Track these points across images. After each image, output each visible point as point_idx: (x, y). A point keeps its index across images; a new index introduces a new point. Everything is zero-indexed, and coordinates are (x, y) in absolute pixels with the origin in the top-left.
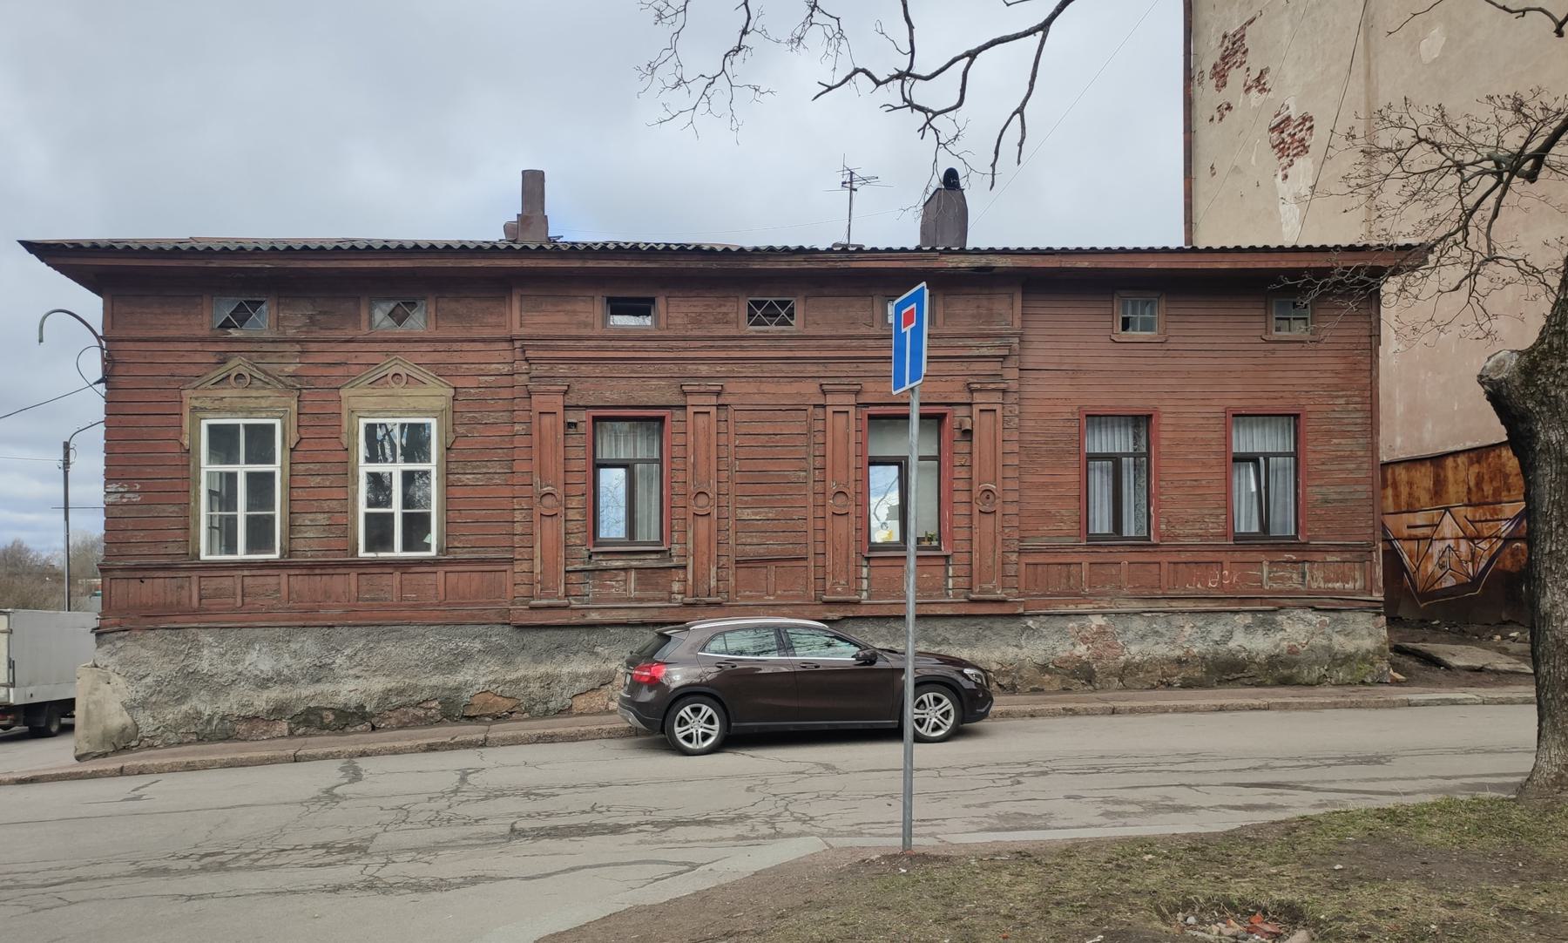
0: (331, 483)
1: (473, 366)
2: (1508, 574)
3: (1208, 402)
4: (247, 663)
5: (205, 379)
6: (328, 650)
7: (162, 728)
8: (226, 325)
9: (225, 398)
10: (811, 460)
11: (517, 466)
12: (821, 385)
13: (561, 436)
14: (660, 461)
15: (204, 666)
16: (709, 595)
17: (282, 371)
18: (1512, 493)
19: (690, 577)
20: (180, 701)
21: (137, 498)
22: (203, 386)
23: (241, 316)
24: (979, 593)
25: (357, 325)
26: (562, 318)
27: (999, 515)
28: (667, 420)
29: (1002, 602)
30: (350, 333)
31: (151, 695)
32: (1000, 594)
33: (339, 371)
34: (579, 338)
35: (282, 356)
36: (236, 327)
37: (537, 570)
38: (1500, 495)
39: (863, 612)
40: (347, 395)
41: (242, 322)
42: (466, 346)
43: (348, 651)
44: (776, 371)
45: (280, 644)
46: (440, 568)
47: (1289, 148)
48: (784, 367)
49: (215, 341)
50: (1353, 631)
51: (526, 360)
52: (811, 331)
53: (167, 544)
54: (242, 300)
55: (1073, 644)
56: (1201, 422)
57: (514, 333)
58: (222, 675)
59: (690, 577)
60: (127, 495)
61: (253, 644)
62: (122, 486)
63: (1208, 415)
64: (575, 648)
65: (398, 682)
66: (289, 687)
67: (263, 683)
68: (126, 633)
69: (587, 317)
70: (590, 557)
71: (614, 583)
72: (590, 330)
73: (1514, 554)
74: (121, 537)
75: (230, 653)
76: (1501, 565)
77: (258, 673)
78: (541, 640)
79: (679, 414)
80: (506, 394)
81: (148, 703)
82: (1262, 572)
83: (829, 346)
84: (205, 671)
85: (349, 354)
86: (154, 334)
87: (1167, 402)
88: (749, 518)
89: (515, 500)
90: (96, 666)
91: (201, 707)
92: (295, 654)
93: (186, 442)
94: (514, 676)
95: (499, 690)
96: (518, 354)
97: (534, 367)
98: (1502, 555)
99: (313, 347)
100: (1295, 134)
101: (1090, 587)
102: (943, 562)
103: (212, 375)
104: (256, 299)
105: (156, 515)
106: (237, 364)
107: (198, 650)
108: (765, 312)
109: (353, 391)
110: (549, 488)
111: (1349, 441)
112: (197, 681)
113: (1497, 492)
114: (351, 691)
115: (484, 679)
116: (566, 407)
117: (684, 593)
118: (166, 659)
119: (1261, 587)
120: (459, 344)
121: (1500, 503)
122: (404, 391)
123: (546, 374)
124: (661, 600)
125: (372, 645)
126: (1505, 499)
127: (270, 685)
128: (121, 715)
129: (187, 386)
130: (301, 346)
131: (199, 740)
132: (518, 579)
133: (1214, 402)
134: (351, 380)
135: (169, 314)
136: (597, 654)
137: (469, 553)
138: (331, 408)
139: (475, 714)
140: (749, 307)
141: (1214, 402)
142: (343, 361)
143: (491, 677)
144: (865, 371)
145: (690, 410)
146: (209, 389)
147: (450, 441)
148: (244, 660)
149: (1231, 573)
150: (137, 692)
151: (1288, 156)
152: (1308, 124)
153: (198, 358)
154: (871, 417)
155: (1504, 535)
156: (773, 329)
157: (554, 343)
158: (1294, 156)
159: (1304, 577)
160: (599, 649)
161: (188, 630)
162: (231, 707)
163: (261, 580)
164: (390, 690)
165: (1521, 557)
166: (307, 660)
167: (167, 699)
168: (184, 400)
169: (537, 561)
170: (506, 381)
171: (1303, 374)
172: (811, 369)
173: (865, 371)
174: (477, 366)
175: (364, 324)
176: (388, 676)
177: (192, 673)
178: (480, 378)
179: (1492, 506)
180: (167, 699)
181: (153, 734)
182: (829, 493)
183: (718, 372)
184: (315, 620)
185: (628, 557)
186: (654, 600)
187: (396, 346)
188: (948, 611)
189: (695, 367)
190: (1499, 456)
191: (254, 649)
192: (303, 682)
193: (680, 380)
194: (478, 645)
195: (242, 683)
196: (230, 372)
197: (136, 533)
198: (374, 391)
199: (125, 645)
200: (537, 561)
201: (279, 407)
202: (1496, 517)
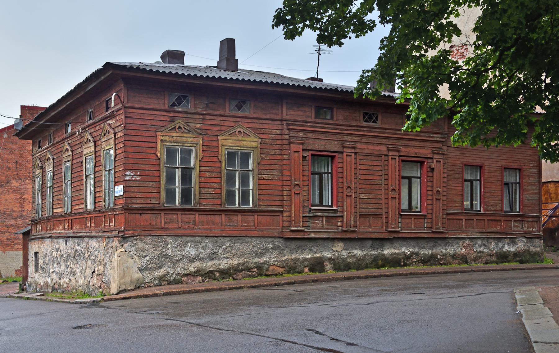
0: (215, 176)
1: (267, 130)
2: (551, 229)
3: (497, 163)
4: (186, 251)
5: (166, 127)
6: (216, 246)
7: (153, 279)
8: (173, 105)
9: (174, 136)
10: (383, 176)
11: (285, 173)
12: (387, 147)
13: (301, 161)
14: (331, 173)
15: (170, 252)
16: (351, 228)
17: (195, 126)
18: (552, 200)
19: (345, 220)
20: (160, 267)
21: (138, 178)
22: (165, 131)
23: (179, 102)
24: (436, 229)
25: (224, 109)
26: (300, 113)
27: (441, 200)
28: (336, 157)
29: (442, 232)
30: (222, 113)
31: (149, 264)
32: (441, 230)
33: (217, 128)
34: (307, 122)
35: (195, 120)
36: (177, 106)
37: (293, 215)
38: (548, 200)
39: (400, 235)
40: (221, 138)
41: (180, 104)
42: (264, 122)
43: (224, 247)
44: (373, 141)
45: (198, 243)
46: (256, 214)
47: (456, 55)
48: (376, 139)
49: (169, 112)
50: (535, 245)
51: (288, 129)
52: (384, 126)
53: (151, 199)
54: (179, 94)
55: (461, 249)
56: (495, 169)
57: (284, 118)
58: (176, 256)
59: (345, 220)
60: (134, 177)
61: (187, 243)
62: (132, 173)
63: (497, 167)
64: (305, 248)
65: (242, 260)
66: (202, 262)
67: (192, 260)
68: (138, 237)
69: (309, 114)
70: (310, 211)
71: (318, 222)
72: (310, 119)
73: (552, 222)
74: (132, 195)
75: (179, 247)
76: (547, 226)
77: (190, 255)
78: (293, 245)
79: (340, 156)
80: (279, 142)
81: (148, 268)
82: (511, 224)
83: (391, 133)
84: (170, 254)
85: (221, 121)
86: (145, 106)
87: (487, 162)
88: (363, 198)
89: (284, 186)
90: (126, 251)
91: (169, 270)
92: (203, 248)
93: (159, 155)
94: (283, 259)
95: (278, 264)
96: (285, 126)
97: (291, 132)
98: (548, 222)
99: (208, 117)
100: (459, 50)
101: (466, 228)
102: (424, 217)
103: (169, 126)
104: (186, 95)
105: (146, 186)
106: (179, 123)
107: (167, 245)
108: (369, 117)
109: (223, 137)
110: (297, 182)
111: (534, 179)
112: (167, 258)
113: (546, 199)
114: (225, 264)
115: (273, 260)
116: (303, 150)
117: (342, 226)
118: (155, 249)
119: (511, 229)
120: (262, 121)
121: (547, 203)
122: (242, 138)
123: (295, 136)
124: (334, 229)
125: (232, 245)
126: (549, 202)
127: (195, 261)
128: (138, 273)
129: (159, 130)
130: (203, 116)
131: (168, 284)
132: (285, 219)
133: (499, 163)
134: (223, 133)
135: (151, 98)
136: (312, 250)
137: (266, 207)
138: (215, 144)
139: (269, 274)
140: (363, 115)
141: (499, 163)
142: (219, 124)
143: (275, 259)
144: (401, 143)
145: (345, 154)
146: (167, 132)
147: (259, 160)
148: (185, 250)
149: (504, 224)
150: (143, 263)
151: (455, 58)
152: (465, 47)
153: (162, 118)
154: (403, 161)
155: (549, 215)
156: (371, 124)
157: (314, 125)
158: (458, 58)
159: (522, 226)
160: (313, 248)
161: (163, 237)
162: (181, 270)
163: (188, 216)
164: (239, 264)
165: (555, 223)
166: (209, 250)
167: (155, 266)
168: (158, 136)
169: (293, 212)
170: (280, 137)
171: (522, 155)
172: (385, 141)
173: (401, 143)
174: (268, 130)
175: (227, 109)
176: (239, 258)
177: (165, 255)
178: (270, 135)
179: (544, 205)
180: (155, 266)
181: (149, 281)
182: (390, 190)
183: (354, 139)
184: (212, 233)
185: (324, 212)
186: (332, 229)
187: (238, 120)
188: (426, 236)
189: (346, 137)
190: (548, 186)
191: (188, 245)
192: (207, 259)
193: (342, 142)
194: (271, 246)
195: (184, 260)
196: (175, 125)
197: (138, 193)
198: (231, 138)
199: (137, 243)
200: (293, 212)
201: (195, 142)
202: (546, 208)
